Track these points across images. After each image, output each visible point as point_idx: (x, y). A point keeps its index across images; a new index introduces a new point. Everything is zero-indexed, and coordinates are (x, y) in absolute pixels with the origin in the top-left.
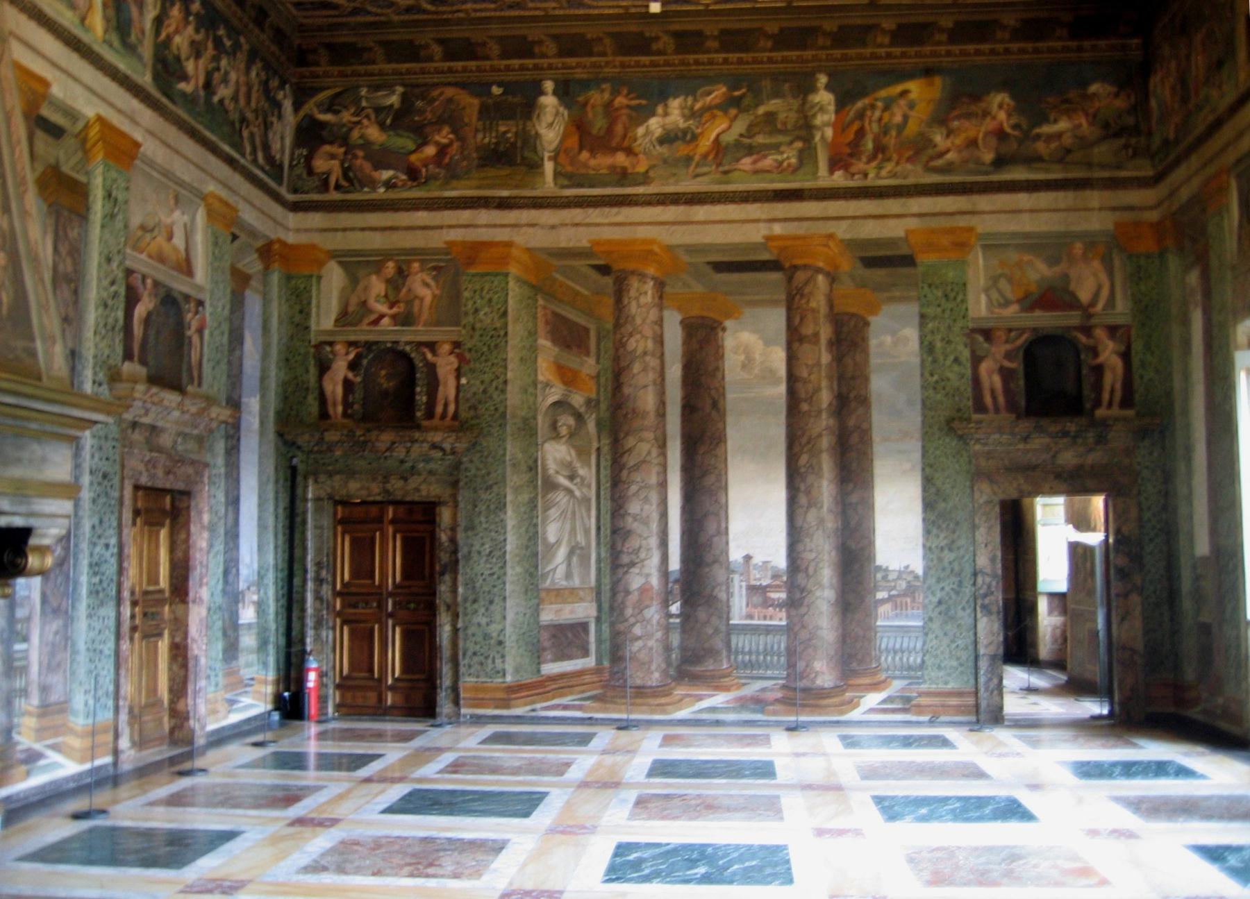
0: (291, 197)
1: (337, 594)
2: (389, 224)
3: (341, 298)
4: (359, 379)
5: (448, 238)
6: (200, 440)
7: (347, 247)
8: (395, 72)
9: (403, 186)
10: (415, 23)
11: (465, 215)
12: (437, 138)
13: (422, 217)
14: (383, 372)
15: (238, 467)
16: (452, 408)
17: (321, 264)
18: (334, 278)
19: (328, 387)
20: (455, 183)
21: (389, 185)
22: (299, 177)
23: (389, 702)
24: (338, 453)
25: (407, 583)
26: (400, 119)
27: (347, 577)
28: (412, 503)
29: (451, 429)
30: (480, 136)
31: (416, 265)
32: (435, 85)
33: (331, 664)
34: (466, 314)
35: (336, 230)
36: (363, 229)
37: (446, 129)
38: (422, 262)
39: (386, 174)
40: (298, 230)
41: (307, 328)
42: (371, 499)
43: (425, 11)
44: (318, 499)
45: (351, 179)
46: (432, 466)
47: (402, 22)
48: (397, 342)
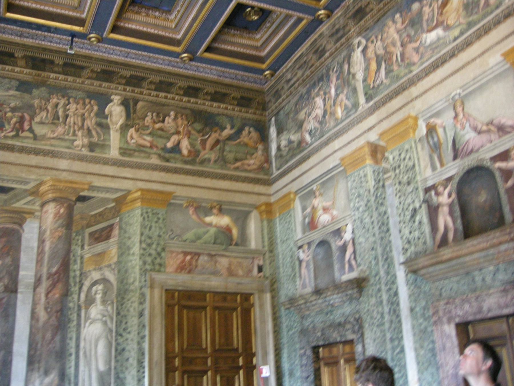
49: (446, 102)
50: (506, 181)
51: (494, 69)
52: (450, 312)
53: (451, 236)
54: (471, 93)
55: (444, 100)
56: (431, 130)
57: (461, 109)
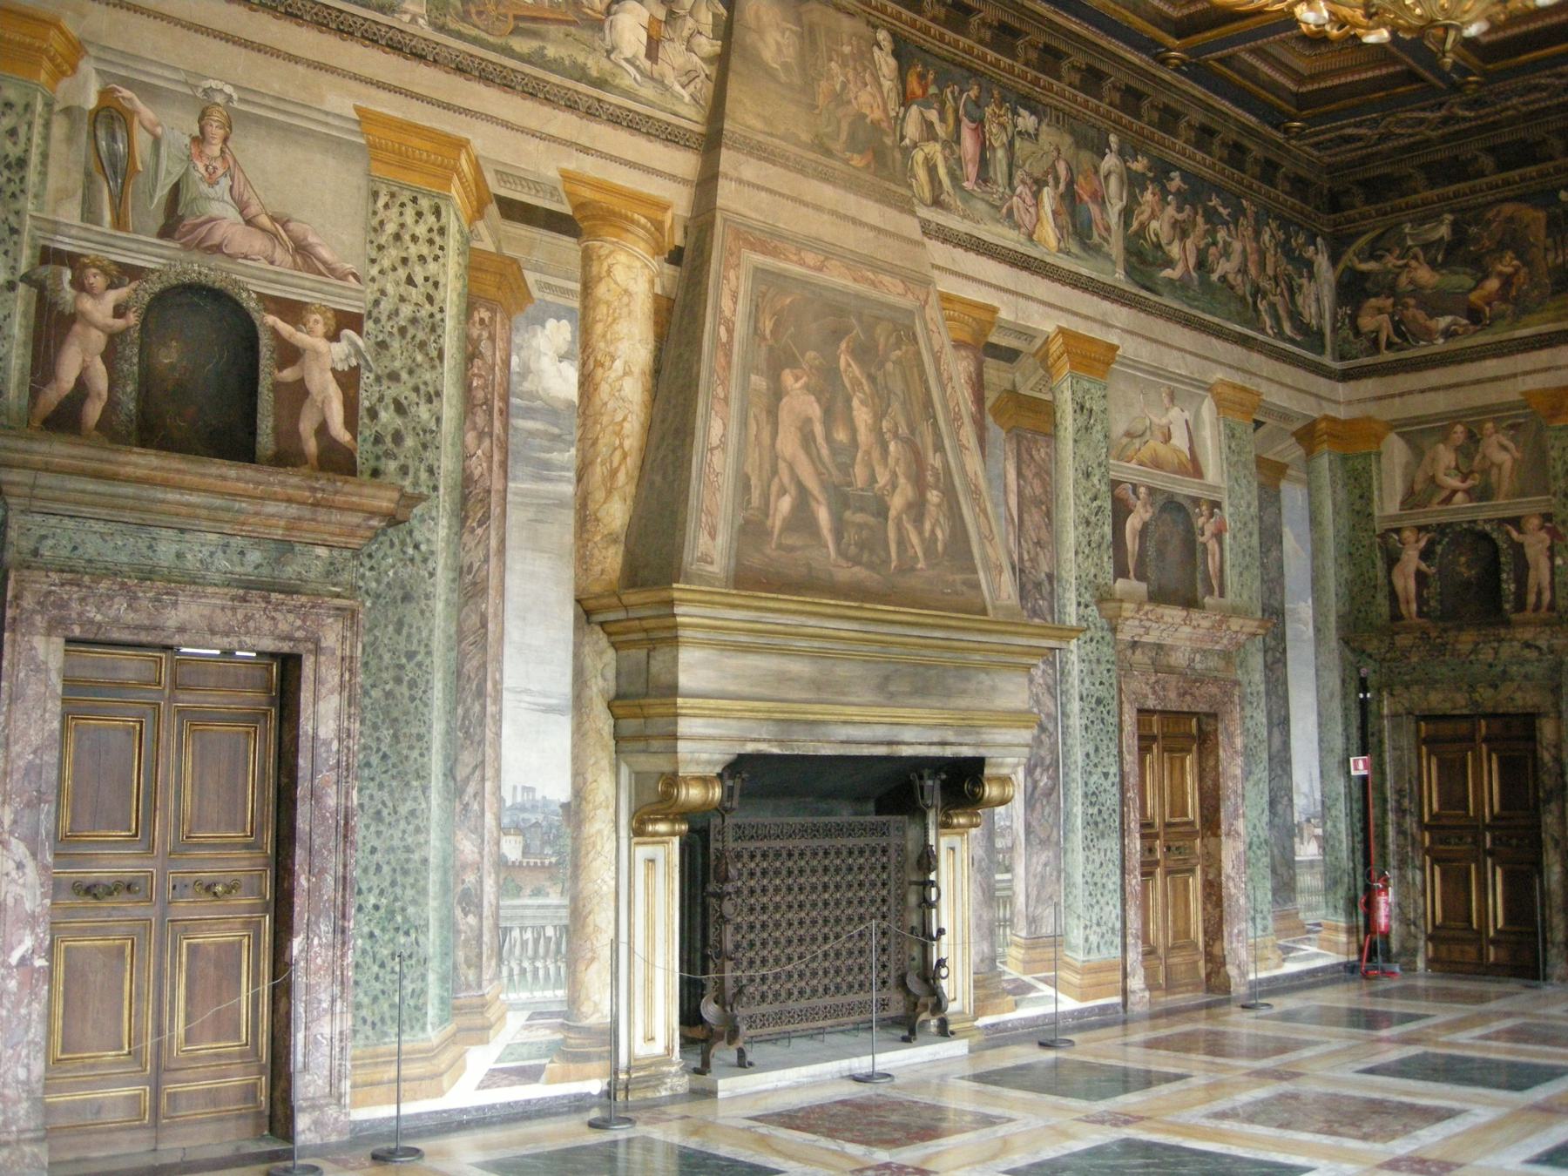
0: (1338, 366)
1: (1423, 826)
2: (1454, 380)
3: (1405, 475)
4: (1433, 570)
5: (1525, 388)
6: (1226, 656)
7: (1406, 415)
8: (1441, 199)
9: (1465, 332)
10: (1456, 135)
11: (1543, 357)
12: (1500, 268)
13: (1491, 366)
14: (1463, 559)
15: (1285, 683)
16: (1547, 596)
17: (1379, 438)
18: (1396, 451)
19: (1399, 584)
20: (1526, 319)
21: (1448, 334)
22: (1345, 340)
23: (1492, 958)
24: (1415, 659)
25: (1506, 813)
26: (1453, 253)
27: (1435, 806)
28: (1504, 715)
29: (1546, 623)
30: (1551, 257)
31: (1489, 425)
32: (1489, 205)
33: (1420, 911)
34: (1555, 478)
35: (1392, 396)
36: (1422, 391)
37: (1509, 255)
38: (1495, 420)
39: (1444, 322)
40: (1349, 403)
41: (1370, 515)
42: (1457, 712)
43: (1464, 119)
44: (1394, 716)
45: (1403, 333)
46: (1529, 668)
47: (1443, 136)
48: (1475, 522)
49: (186, 83)
50: (281, 368)
51: (330, 120)
52: (63, 605)
53: (93, 411)
54: (258, 120)
55: (182, 77)
56: (111, 115)
57: (221, 132)
